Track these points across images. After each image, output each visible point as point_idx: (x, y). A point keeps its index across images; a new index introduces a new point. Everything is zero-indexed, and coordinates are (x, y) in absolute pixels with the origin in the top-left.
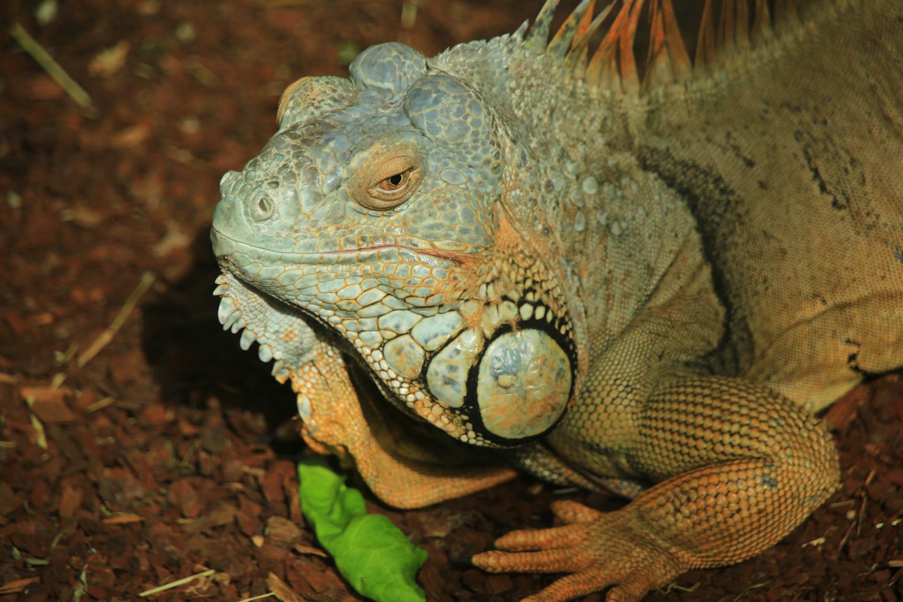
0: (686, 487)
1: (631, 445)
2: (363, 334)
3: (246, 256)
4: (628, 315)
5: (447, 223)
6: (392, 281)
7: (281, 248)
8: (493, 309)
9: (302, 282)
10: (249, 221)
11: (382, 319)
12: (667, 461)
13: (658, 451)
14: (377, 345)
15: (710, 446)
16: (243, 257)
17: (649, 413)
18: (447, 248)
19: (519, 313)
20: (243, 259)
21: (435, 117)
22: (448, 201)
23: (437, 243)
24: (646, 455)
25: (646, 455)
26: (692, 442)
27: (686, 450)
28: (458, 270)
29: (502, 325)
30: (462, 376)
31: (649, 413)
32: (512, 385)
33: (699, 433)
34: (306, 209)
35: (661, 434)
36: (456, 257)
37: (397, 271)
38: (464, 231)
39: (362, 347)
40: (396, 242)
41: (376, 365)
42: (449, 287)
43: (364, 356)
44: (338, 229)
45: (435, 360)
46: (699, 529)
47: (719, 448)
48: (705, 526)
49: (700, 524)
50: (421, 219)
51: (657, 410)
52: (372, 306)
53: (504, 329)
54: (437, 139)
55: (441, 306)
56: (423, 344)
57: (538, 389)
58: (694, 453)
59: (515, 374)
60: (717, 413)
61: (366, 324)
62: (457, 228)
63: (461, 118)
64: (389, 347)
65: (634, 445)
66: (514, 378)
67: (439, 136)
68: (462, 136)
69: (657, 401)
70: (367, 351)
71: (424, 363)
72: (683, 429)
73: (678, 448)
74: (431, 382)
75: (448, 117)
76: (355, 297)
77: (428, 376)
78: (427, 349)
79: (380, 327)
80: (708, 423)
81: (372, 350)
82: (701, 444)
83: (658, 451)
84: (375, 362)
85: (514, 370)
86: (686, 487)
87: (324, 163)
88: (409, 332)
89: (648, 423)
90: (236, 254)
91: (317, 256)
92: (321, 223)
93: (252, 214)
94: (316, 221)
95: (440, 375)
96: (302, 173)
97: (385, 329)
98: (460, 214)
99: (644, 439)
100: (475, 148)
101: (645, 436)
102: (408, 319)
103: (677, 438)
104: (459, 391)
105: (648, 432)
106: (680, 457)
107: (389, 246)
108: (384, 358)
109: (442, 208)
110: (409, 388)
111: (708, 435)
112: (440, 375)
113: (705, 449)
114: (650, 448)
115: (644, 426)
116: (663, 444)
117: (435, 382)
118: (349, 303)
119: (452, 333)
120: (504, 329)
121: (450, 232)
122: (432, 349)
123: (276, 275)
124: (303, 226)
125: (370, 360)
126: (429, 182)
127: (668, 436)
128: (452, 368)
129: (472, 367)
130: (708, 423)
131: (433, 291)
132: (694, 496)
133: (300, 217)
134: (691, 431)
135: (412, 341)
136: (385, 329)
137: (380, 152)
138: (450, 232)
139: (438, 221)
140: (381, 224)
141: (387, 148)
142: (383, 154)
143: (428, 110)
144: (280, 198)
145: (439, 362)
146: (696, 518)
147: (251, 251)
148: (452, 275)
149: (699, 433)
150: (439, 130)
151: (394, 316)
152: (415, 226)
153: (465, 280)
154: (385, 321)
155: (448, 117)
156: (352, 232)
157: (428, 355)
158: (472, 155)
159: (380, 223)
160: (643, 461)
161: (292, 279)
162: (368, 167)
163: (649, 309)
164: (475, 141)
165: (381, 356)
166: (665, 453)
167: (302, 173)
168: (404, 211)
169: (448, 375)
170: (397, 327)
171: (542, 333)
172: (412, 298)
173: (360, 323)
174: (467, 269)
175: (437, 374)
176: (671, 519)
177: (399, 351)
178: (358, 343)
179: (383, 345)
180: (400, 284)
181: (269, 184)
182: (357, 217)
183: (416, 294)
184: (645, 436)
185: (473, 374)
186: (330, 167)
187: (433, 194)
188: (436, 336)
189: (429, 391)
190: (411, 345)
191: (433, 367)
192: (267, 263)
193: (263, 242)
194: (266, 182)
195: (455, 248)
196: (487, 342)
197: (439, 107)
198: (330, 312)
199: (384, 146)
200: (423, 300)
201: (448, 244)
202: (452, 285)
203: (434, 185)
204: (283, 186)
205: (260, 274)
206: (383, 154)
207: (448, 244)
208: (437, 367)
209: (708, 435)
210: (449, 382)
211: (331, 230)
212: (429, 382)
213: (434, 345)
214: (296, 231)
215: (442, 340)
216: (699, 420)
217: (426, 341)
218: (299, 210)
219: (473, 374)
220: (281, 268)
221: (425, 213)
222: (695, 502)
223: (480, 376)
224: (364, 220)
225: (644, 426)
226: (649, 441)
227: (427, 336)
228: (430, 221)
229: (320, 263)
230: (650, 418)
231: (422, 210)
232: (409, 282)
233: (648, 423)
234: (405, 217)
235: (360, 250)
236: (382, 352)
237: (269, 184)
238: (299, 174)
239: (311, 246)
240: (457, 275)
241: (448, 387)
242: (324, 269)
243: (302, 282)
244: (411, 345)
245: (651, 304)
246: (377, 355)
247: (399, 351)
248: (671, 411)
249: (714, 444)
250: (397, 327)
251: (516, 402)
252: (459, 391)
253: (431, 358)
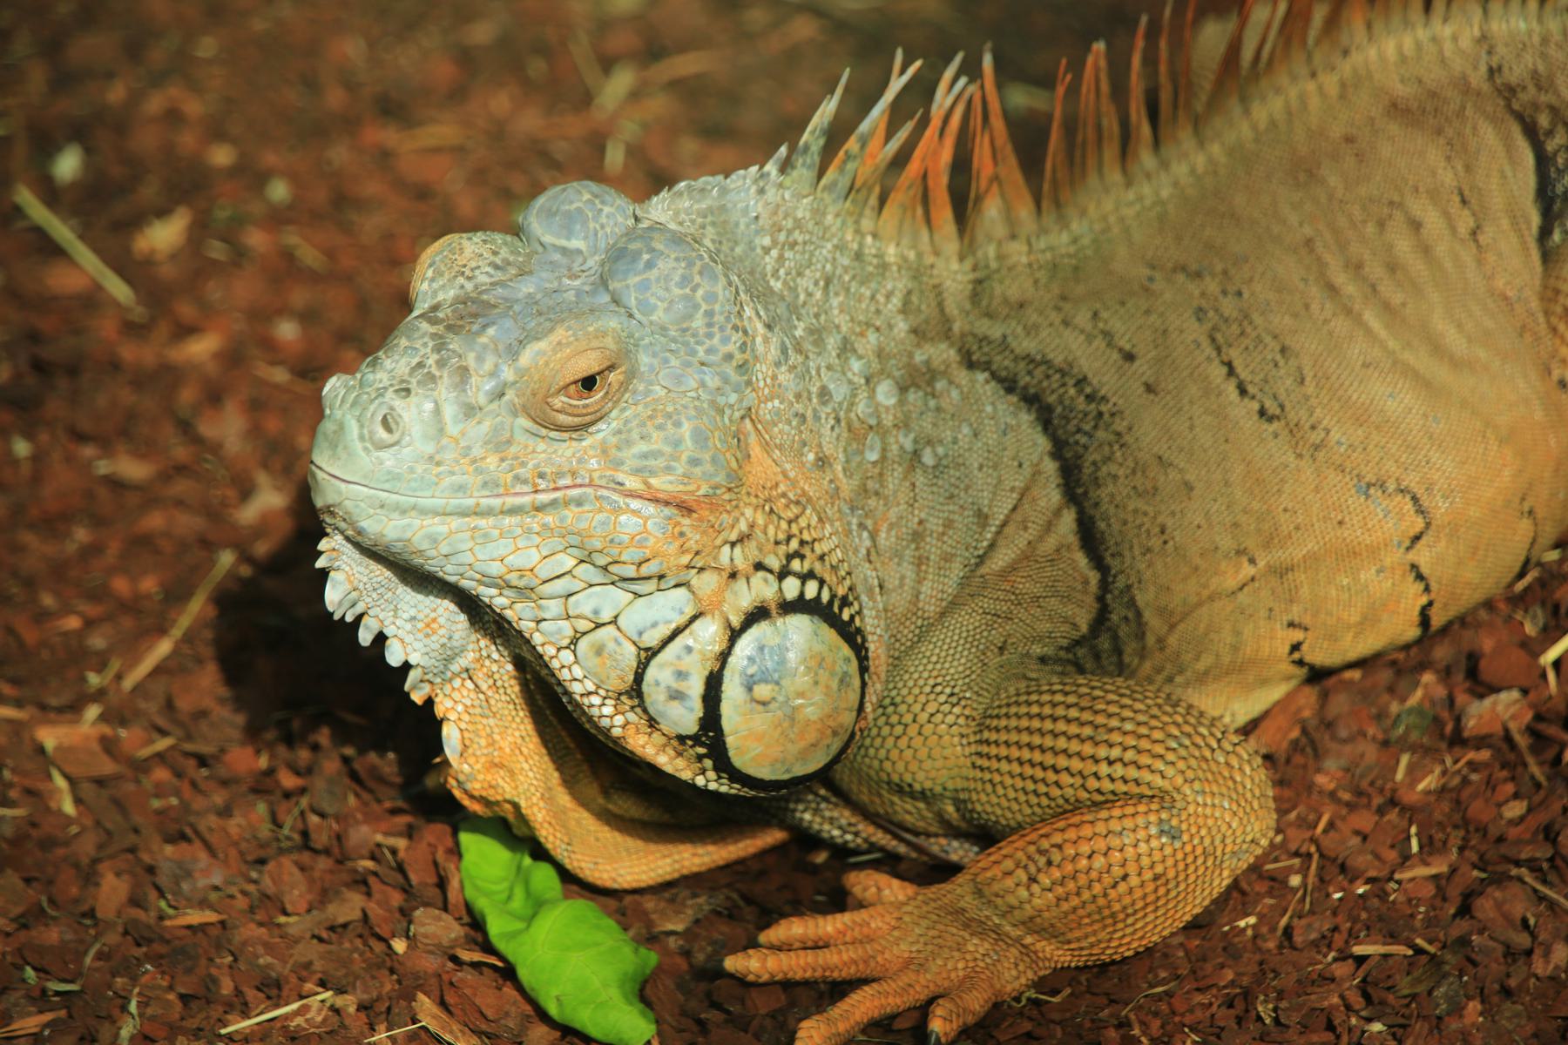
0: (1045, 844)
1: (960, 784)
2: (544, 623)
3: (362, 504)
4: (951, 585)
5: (667, 449)
6: (586, 540)
7: (415, 490)
8: (741, 584)
9: (449, 544)
10: (366, 449)
11: (572, 599)
12: (1015, 807)
13: (1001, 791)
14: (566, 642)
15: (1078, 781)
16: (357, 506)
17: (986, 735)
18: (670, 488)
19: (780, 589)
20: (358, 510)
21: (647, 288)
22: (669, 416)
23: (653, 481)
24: (984, 798)
25: (984, 798)
26: (1052, 777)
27: (1042, 789)
28: (686, 521)
29: (756, 607)
30: (696, 687)
31: (986, 735)
32: (774, 699)
33: (1062, 762)
34: (453, 429)
35: (1004, 766)
36: (683, 502)
37: (593, 524)
38: (694, 462)
39: (543, 645)
40: (591, 480)
41: (565, 671)
42: (673, 548)
43: (546, 658)
44: (502, 460)
45: (654, 663)
46: (1065, 906)
47: (1093, 784)
48: (1075, 901)
49: (1066, 900)
50: (629, 443)
51: (997, 730)
52: (556, 581)
53: (758, 614)
54: (651, 323)
55: (661, 577)
56: (635, 638)
57: (812, 704)
58: (1056, 792)
59: (777, 683)
60: (1087, 731)
61: (548, 608)
62: (684, 457)
63: (687, 291)
64: (583, 644)
65: (965, 784)
66: (777, 688)
67: (654, 318)
68: (690, 317)
69: (998, 717)
70: (549, 651)
71: (638, 667)
72: (1037, 757)
73: (1030, 786)
74: (649, 695)
75: (667, 289)
76: (529, 566)
77: (645, 688)
78: (642, 646)
79: (571, 614)
80: (1074, 746)
81: (559, 650)
82: (1065, 779)
83: (1001, 791)
84: (563, 667)
85: (776, 676)
86: (1045, 844)
87: (480, 359)
88: (614, 621)
89: (985, 749)
90: (347, 502)
91: (470, 502)
92: (477, 451)
93: (371, 438)
94: (469, 448)
95: (663, 685)
96: (445, 375)
97: (577, 617)
98: (687, 436)
99: (979, 774)
100: (710, 336)
101: (982, 769)
102: (610, 600)
103: (1029, 771)
104: (692, 710)
105: (985, 763)
106: (1034, 800)
107: (581, 486)
108: (577, 662)
109: (660, 427)
110: (615, 706)
111: (1076, 764)
112: (663, 685)
113: (1072, 785)
114: (989, 787)
115: (979, 754)
116: (1009, 781)
117: (655, 695)
118: (522, 576)
119: (680, 620)
120: (758, 614)
121: (672, 463)
122: (649, 645)
123: (408, 535)
124: (449, 456)
125: (555, 664)
126: (641, 388)
127: (1016, 768)
128: (681, 675)
129: (711, 673)
130: (1074, 746)
131: (648, 553)
132: (1056, 856)
133: (444, 441)
134: (1049, 759)
135: (617, 633)
136: (577, 617)
137: (564, 341)
138: (672, 463)
139: (654, 447)
140: (569, 453)
141: (574, 335)
142: (569, 344)
143: (637, 279)
144: (413, 413)
145: (661, 666)
146: (1060, 890)
147: (370, 497)
148: (677, 529)
149: (1062, 762)
150: (655, 307)
151: (590, 596)
152: (620, 454)
153: (698, 537)
154: (577, 602)
155: (667, 289)
156: (523, 464)
157: (643, 654)
158: (705, 347)
159: (566, 451)
160: (979, 808)
161: (434, 540)
162: (547, 364)
163: (982, 576)
164: (710, 325)
165: (572, 658)
166: (1012, 794)
167: (445, 375)
168: (603, 431)
169: (675, 685)
170: (596, 612)
171: (816, 619)
172: (616, 566)
173: (540, 607)
174: (700, 520)
175: (657, 684)
176: (1023, 893)
177: (599, 650)
178: (537, 639)
179: (574, 642)
180: (598, 544)
181: (397, 391)
182: (531, 441)
183: (623, 558)
184: (982, 769)
185: (714, 685)
186: (488, 365)
187: (646, 406)
188: (654, 625)
189: (645, 711)
190: (616, 641)
191: (652, 673)
192: (395, 515)
193: (387, 481)
194: (391, 389)
195: (681, 488)
196: (735, 635)
197: (653, 274)
198: (494, 591)
199: (571, 332)
200: (634, 567)
201: (671, 483)
202: (677, 544)
203: (648, 392)
204: (417, 394)
205: (385, 532)
206: (569, 344)
207: (671, 483)
208: (657, 673)
209: (1076, 764)
210: (677, 696)
211: (492, 461)
212: (645, 696)
213: (652, 639)
214: (438, 464)
215: (664, 631)
216: (1062, 743)
217: (640, 634)
218: (441, 430)
219: (714, 685)
220: (417, 522)
221: (635, 435)
222: (1059, 866)
223: (724, 687)
224: (542, 446)
225: (979, 754)
226: (987, 776)
227: (640, 627)
228: (643, 447)
229: (476, 514)
230: (988, 743)
231: (629, 431)
232: (612, 541)
233: (985, 749)
234: (604, 441)
235: (536, 492)
236: (574, 652)
237: (397, 391)
238: (441, 377)
239: (461, 488)
240: (684, 529)
241: (675, 704)
242: (482, 522)
243: (449, 544)
244: (616, 641)
245: (983, 570)
246: (567, 657)
247: (599, 650)
248: (1018, 730)
249: (1084, 778)
250: (596, 612)
251: (780, 725)
252: (692, 710)
253: (648, 660)
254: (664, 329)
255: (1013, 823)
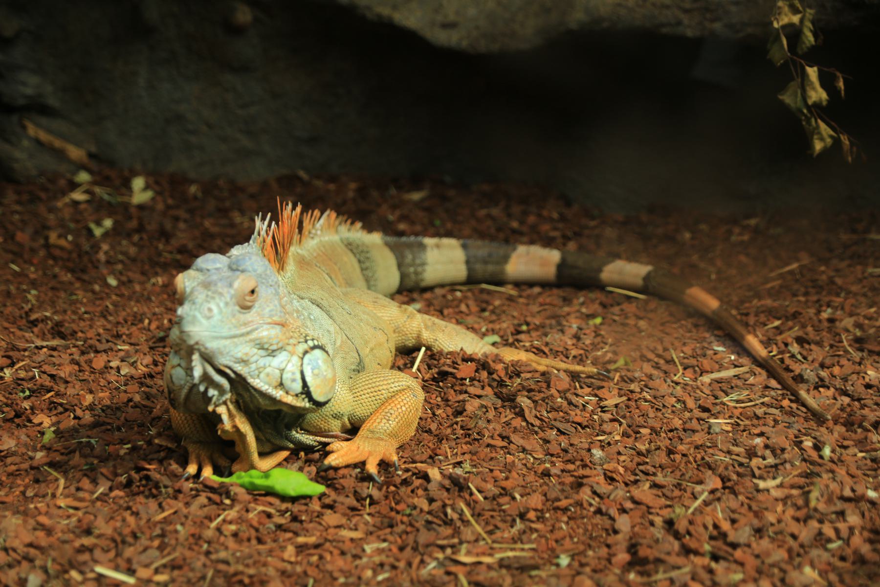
0: (387, 410)
46: (399, 424)
48: (401, 422)
72: (373, 390)
80: (381, 383)
86: (387, 410)
111: (385, 387)
117: (287, 383)
130: (381, 383)
132: (393, 412)
134: (377, 389)
146: (397, 420)
149: (381, 388)
166: (368, 404)
191: (285, 376)
209: (385, 387)
216: (378, 384)
254: (261, 275)
255: (369, 414)
